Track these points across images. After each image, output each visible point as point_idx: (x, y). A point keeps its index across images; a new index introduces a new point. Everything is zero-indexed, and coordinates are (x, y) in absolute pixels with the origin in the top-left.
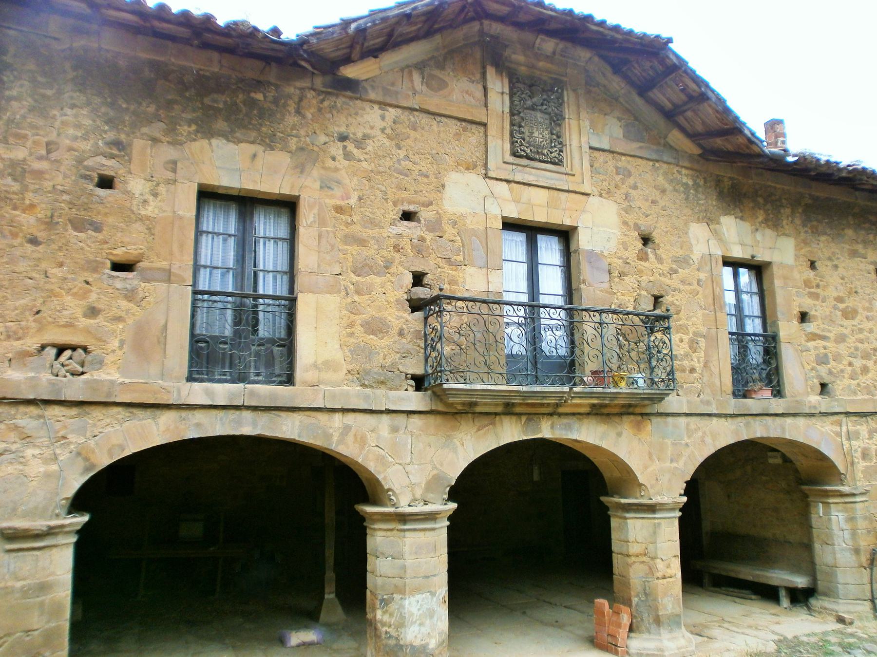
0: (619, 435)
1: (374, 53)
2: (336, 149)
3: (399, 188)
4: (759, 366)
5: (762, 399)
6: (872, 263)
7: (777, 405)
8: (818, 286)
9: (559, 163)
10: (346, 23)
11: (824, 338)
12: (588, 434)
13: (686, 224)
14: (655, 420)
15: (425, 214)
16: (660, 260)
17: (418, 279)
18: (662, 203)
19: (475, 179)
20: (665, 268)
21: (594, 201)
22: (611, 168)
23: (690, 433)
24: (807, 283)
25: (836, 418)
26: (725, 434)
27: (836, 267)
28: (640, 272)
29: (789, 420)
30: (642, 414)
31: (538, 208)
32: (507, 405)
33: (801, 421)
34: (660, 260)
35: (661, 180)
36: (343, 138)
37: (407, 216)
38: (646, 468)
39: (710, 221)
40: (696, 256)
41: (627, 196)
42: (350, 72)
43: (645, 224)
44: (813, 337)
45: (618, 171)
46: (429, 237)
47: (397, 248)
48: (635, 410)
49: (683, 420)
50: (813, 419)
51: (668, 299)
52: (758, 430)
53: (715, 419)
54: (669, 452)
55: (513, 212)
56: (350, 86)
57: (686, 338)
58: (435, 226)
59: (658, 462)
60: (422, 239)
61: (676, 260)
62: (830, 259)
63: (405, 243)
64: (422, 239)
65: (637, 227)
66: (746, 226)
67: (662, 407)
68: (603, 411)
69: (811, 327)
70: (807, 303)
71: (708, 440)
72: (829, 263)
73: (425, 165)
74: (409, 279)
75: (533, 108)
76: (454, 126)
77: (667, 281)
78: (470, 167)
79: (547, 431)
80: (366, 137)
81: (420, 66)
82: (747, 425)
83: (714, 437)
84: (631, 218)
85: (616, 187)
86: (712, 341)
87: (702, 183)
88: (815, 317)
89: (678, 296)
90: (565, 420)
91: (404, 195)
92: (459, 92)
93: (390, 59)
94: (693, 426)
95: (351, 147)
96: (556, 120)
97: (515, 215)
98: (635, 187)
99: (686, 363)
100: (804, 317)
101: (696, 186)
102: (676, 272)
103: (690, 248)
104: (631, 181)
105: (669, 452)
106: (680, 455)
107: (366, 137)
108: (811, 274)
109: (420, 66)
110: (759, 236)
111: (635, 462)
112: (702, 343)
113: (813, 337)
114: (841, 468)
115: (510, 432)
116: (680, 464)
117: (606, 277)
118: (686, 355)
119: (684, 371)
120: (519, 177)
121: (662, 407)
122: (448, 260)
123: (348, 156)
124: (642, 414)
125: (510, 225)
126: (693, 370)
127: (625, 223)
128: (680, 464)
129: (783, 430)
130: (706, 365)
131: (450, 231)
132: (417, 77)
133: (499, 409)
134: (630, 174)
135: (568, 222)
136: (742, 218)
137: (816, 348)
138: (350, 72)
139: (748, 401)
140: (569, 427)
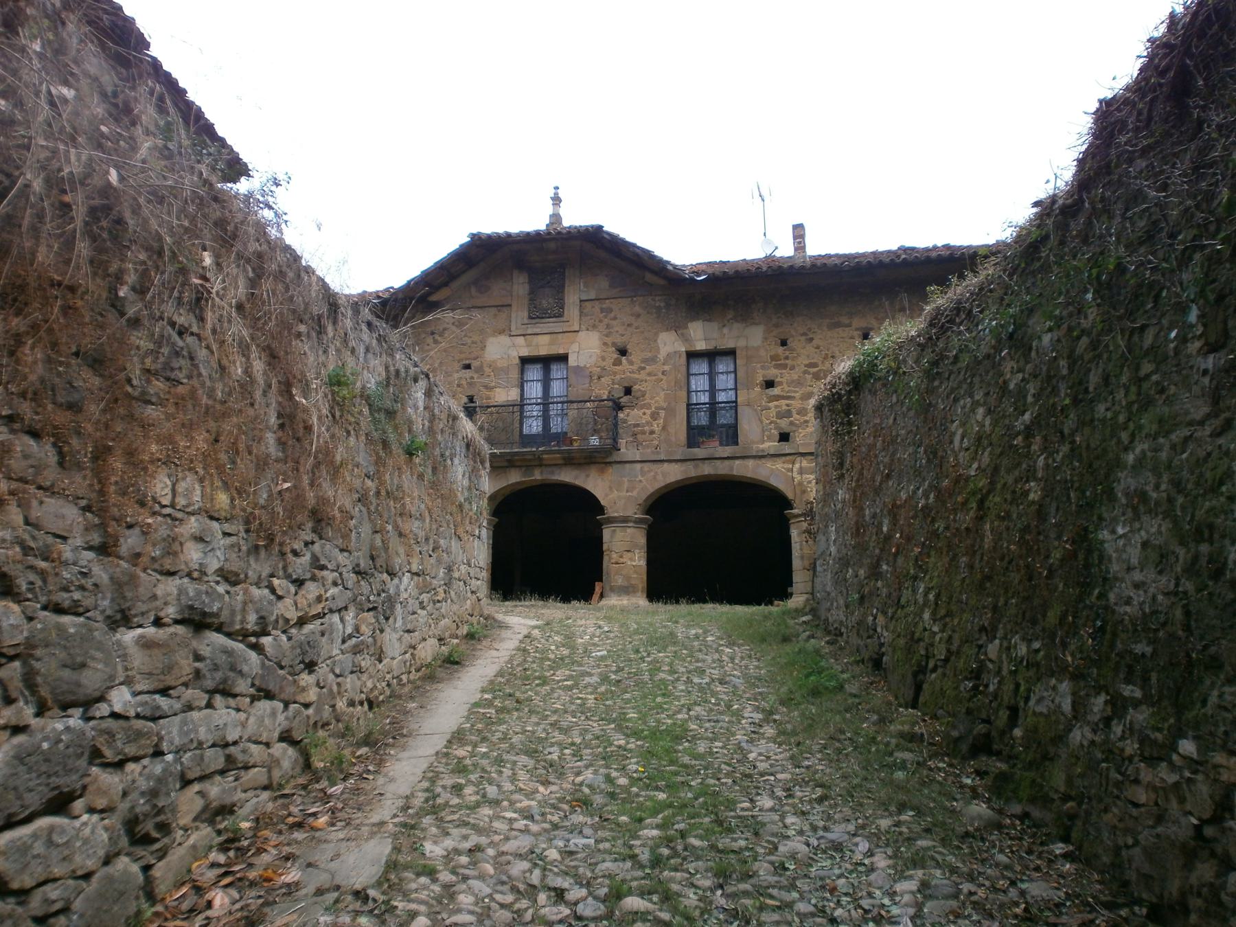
0: (588, 476)
1: (446, 284)
2: (430, 340)
3: (461, 353)
4: (713, 426)
5: (715, 448)
6: (857, 329)
7: (728, 451)
8: (787, 358)
9: (561, 315)
10: (409, 282)
11: (788, 398)
12: (567, 476)
13: (656, 334)
14: (616, 466)
15: (475, 364)
16: (631, 363)
17: (471, 399)
18: (636, 324)
19: (504, 340)
20: (635, 367)
21: (582, 334)
22: (597, 309)
23: (643, 473)
24: (774, 358)
25: (788, 458)
26: (673, 474)
27: (811, 340)
28: (615, 374)
29: (737, 462)
30: (606, 463)
31: (543, 346)
32: (509, 461)
33: (751, 463)
34: (631, 363)
35: (637, 309)
36: (433, 333)
37: (468, 367)
38: (607, 495)
39: (678, 328)
40: (662, 354)
41: (608, 326)
42: (433, 298)
43: (619, 341)
44: (778, 398)
45: (602, 310)
46: (476, 376)
47: (458, 386)
48: (600, 459)
49: (638, 466)
50: (763, 461)
51: (636, 387)
52: (707, 469)
53: (666, 465)
54: (626, 485)
55: (525, 352)
56: (434, 306)
57: (648, 412)
58: (480, 370)
59: (621, 492)
60: (472, 378)
61: (645, 361)
62: (804, 334)
63: (464, 382)
64: (472, 378)
65: (614, 344)
66: (714, 326)
67: (615, 457)
68: (570, 461)
69: (776, 391)
70: (772, 373)
71: (660, 477)
72: (803, 338)
73: (476, 338)
74: (465, 400)
75: (542, 287)
76: (494, 310)
77: (636, 376)
78: (501, 332)
79: (538, 476)
80: (445, 329)
81: (475, 282)
82: (696, 467)
83: (664, 475)
84: (609, 340)
85: (601, 321)
86: (670, 411)
87: (673, 302)
88: (781, 383)
89: (645, 385)
90: (550, 469)
91: (463, 356)
92: (497, 290)
93: (455, 285)
94: (646, 469)
95: (437, 337)
96: (560, 289)
97: (526, 354)
98: (615, 318)
99: (646, 428)
100: (770, 384)
101: (668, 306)
102: (644, 368)
103: (658, 350)
104: (612, 315)
105: (626, 485)
106: (634, 488)
107: (445, 329)
108: (780, 350)
109: (475, 282)
110: (725, 330)
111: (598, 493)
112: (662, 414)
113: (778, 398)
114: (790, 495)
115: (514, 477)
116: (635, 493)
117: (587, 380)
118: (648, 423)
119: (644, 433)
120: (529, 331)
121: (615, 457)
122: (486, 387)
123: (436, 342)
124: (606, 463)
125: (525, 361)
126: (652, 432)
127: (605, 344)
128: (635, 493)
129: (732, 468)
130: (664, 428)
131: (487, 370)
132: (473, 290)
133: (506, 464)
134: (611, 311)
135: (561, 351)
136: (709, 320)
137: (776, 407)
138: (433, 298)
139: (696, 450)
140: (552, 473)
